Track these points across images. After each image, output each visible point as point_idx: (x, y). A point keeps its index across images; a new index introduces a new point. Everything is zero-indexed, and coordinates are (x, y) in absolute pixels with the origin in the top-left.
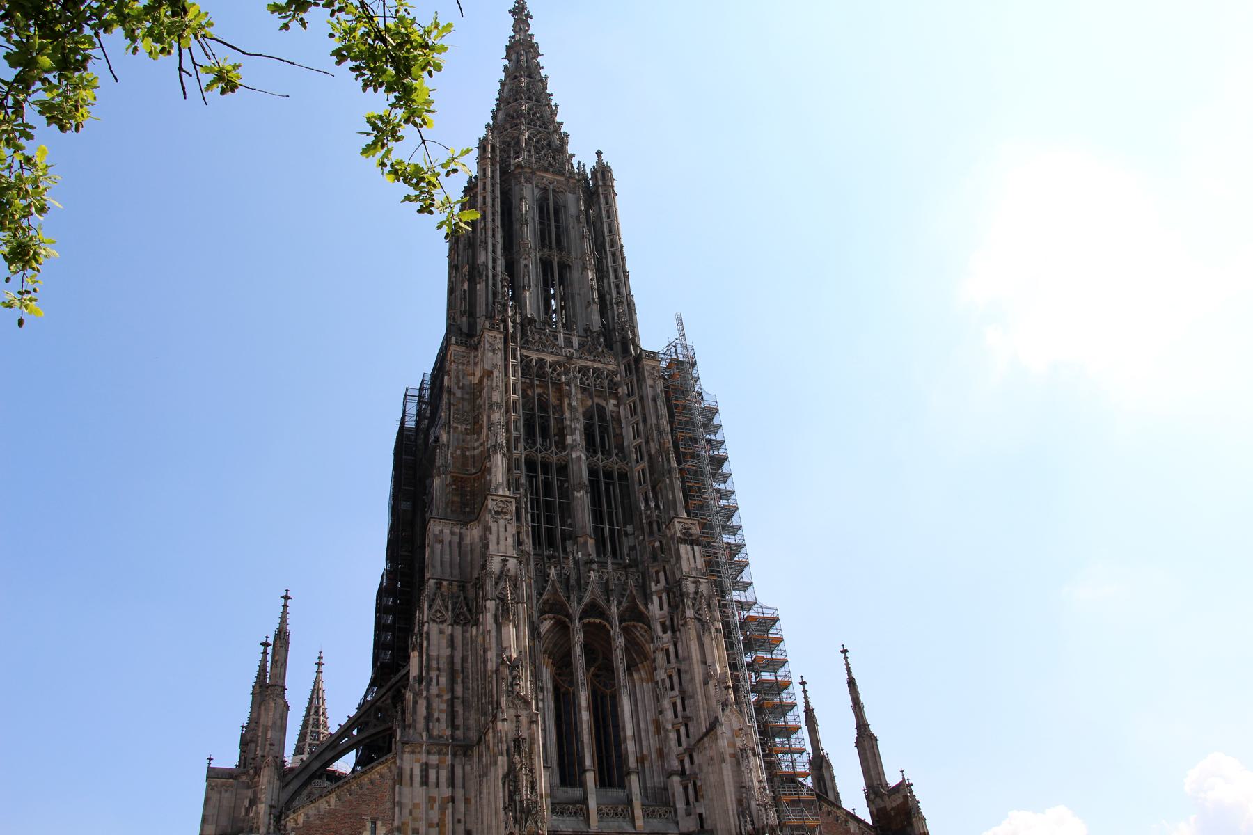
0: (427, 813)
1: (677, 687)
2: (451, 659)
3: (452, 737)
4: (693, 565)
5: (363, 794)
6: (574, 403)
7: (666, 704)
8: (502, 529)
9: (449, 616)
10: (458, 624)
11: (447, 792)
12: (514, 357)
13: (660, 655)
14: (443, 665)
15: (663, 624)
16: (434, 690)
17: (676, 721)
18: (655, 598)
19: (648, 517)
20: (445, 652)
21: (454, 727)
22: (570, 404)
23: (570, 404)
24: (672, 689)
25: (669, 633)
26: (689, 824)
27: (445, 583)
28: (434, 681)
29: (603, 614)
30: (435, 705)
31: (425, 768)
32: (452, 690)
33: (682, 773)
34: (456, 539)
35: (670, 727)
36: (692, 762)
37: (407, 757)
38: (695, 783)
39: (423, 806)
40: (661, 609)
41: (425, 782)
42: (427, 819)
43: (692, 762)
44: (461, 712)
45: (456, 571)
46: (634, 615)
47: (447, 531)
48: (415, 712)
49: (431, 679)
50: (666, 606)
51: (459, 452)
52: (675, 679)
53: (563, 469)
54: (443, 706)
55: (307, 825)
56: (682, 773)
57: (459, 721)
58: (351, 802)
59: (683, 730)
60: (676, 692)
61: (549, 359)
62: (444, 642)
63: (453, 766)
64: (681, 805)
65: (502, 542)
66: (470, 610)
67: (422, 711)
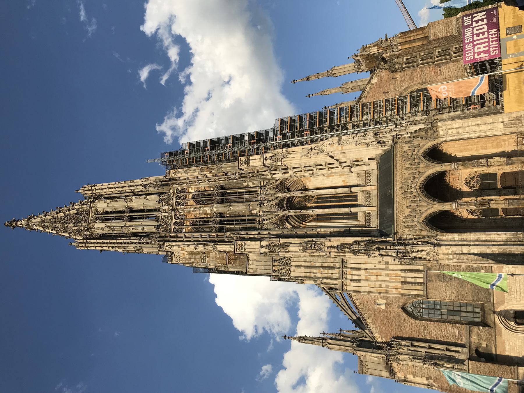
0: (372, 281)
1: (312, 168)
2: (305, 267)
3: (339, 268)
4: (258, 160)
5: (365, 307)
6: (192, 209)
7: (320, 172)
8: (249, 247)
9: (287, 268)
10: (290, 263)
11: (362, 272)
12: (174, 237)
13: (298, 174)
14: (308, 270)
15: (285, 173)
16: (319, 275)
17: (327, 169)
18: (274, 176)
19: (239, 178)
20: (302, 270)
21: (333, 268)
22: (193, 211)
23: (193, 211)
24: (313, 170)
25: (289, 171)
26: (374, 165)
27: (274, 269)
28: (315, 274)
29: (282, 200)
30: (326, 275)
31: (352, 280)
32: (319, 267)
33: (351, 167)
34: (255, 263)
35: (330, 172)
36: (345, 162)
37: (348, 288)
38: (354, 161)
39: (369, 283)
40: (278, 174)
41: (359, 281)
42: (375, 281)
43: (345, 162)
44: (328, 264)
45: (269, 263)
46: (282, 186)
47: (252, 267)
48: (329, 284)
49: (315, 276)
50: (277, 172)
51: (218, 260)
52: (308, 168)
53: (221, 215)
54: (326, 271)
55: (380, 333)
56: (351, 167)
57: (332, 265)
58: (369, 314)
59: (331, 166)
60: (315, 169)
61: (174, 220)
62: (299, 270)
63: (351, 268)
64: (365, 168)
65: (254, 247)
66: (284, 258)
67: (328, 281)
